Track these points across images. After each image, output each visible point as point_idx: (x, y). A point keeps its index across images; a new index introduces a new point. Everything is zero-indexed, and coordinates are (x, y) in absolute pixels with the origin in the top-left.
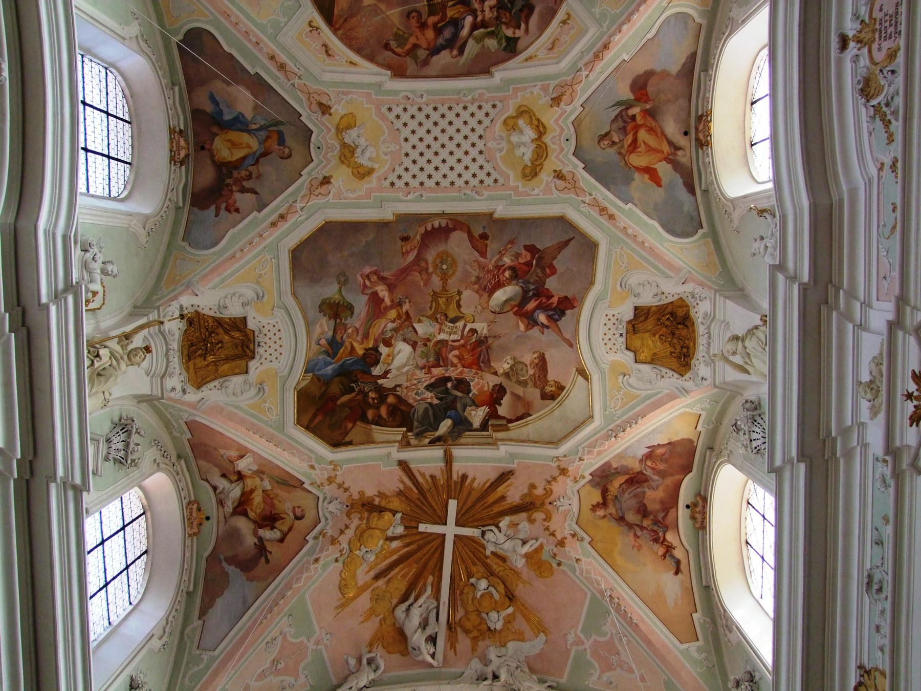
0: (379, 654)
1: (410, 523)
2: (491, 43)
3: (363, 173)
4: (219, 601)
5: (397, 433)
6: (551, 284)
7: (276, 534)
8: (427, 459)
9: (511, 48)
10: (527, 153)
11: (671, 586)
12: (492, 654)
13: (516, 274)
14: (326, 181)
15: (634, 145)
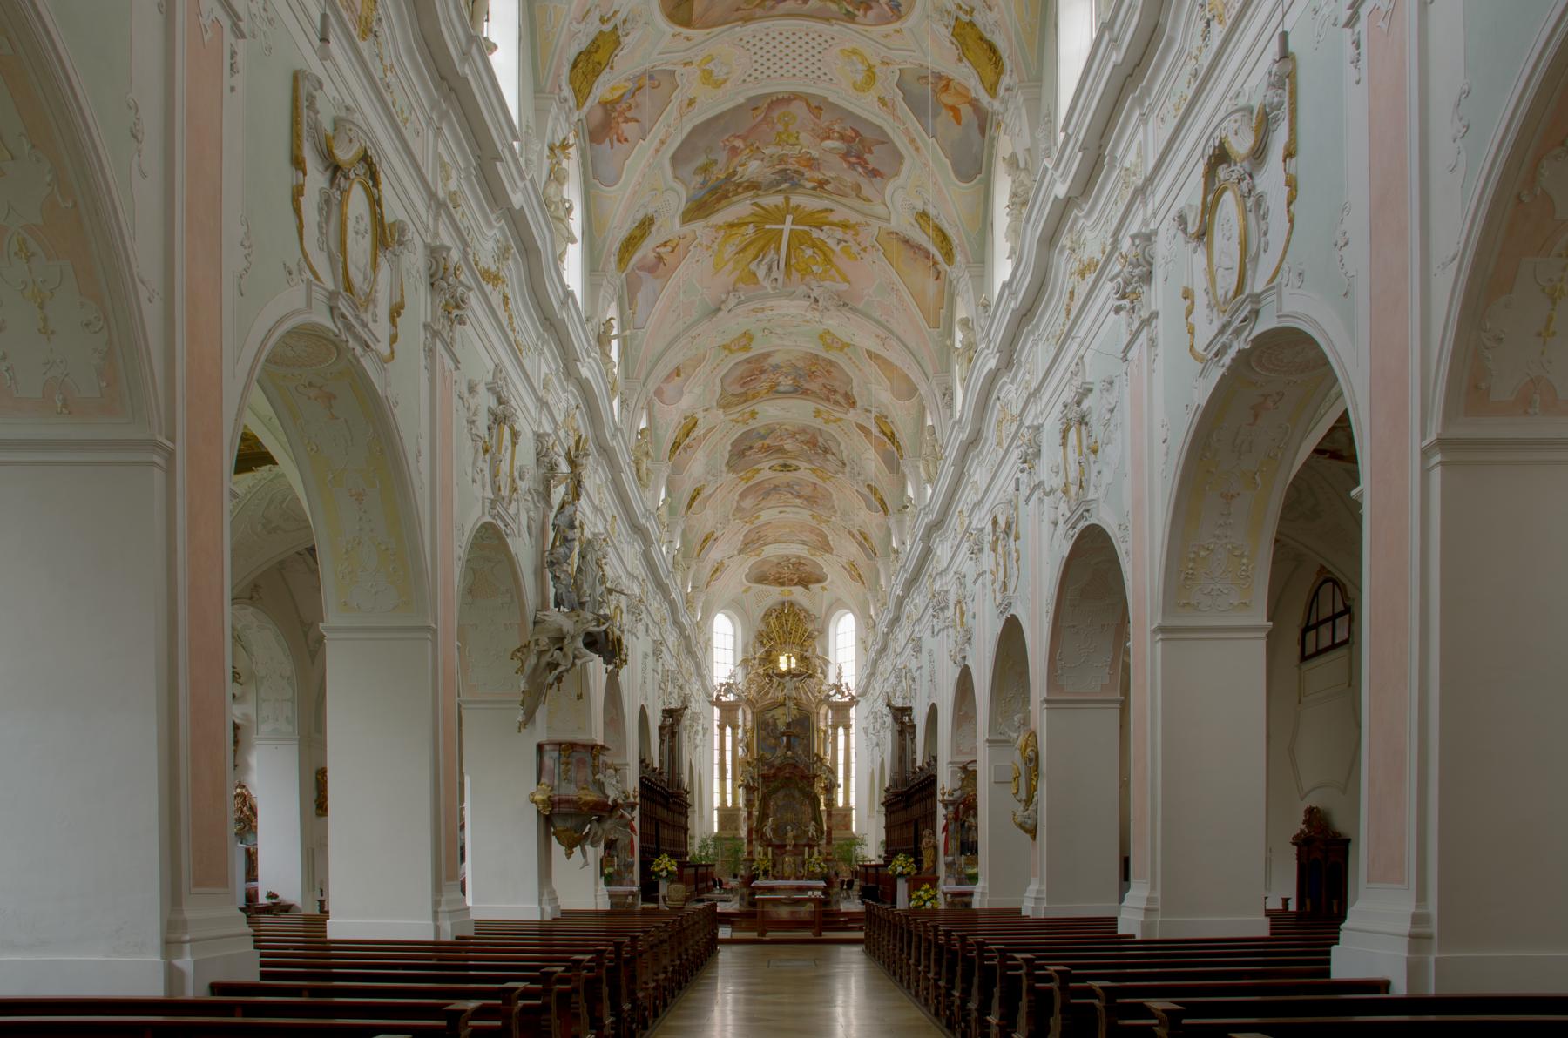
0: (740, 285)
1: (758, 228)
2: (834, 7)
3: (718, 85)
4: (639, 295)
5: (751, 193)
6: (867, 156)
7: (669, 249)
8: (772, 200)
9: (851, 17)
10: (859, 78)
11: (931, 286)
12: (814, 284)
13: (842, 137)
14: (691, 102)
15: (947, 87)
